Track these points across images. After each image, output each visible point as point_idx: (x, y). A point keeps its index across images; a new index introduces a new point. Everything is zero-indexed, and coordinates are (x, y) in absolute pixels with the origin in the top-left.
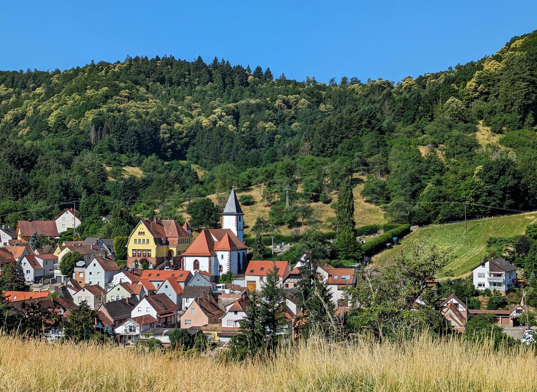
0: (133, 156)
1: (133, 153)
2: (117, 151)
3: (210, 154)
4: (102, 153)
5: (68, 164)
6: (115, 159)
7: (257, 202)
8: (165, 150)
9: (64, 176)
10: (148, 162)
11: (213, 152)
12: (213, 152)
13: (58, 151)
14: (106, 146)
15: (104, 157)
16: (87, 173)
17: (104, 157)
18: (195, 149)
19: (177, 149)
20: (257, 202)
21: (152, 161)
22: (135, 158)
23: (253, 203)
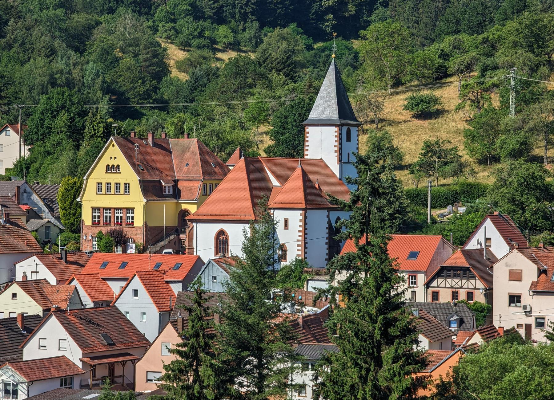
0: (244, 30)
1: (245, 22)
2: (209, 17)
3: (422, 25)
4: (174, 21)
5: (78, 41)
6: (200, 35)
7: (448, 112)
8: (321, 16)
9: (59, 64)
10: (273, 40)
11: (428, 20)
12: (428, 20)
13: (60, 12)
14: (185, 7)
15: (176, 31)
16: (118, 59)
17: (176, 31)
18: (388, 13)
19: (347, 15)
20: (448, 112)
21: (284, 39)
22: (249, 33)
23: (438, 114)
